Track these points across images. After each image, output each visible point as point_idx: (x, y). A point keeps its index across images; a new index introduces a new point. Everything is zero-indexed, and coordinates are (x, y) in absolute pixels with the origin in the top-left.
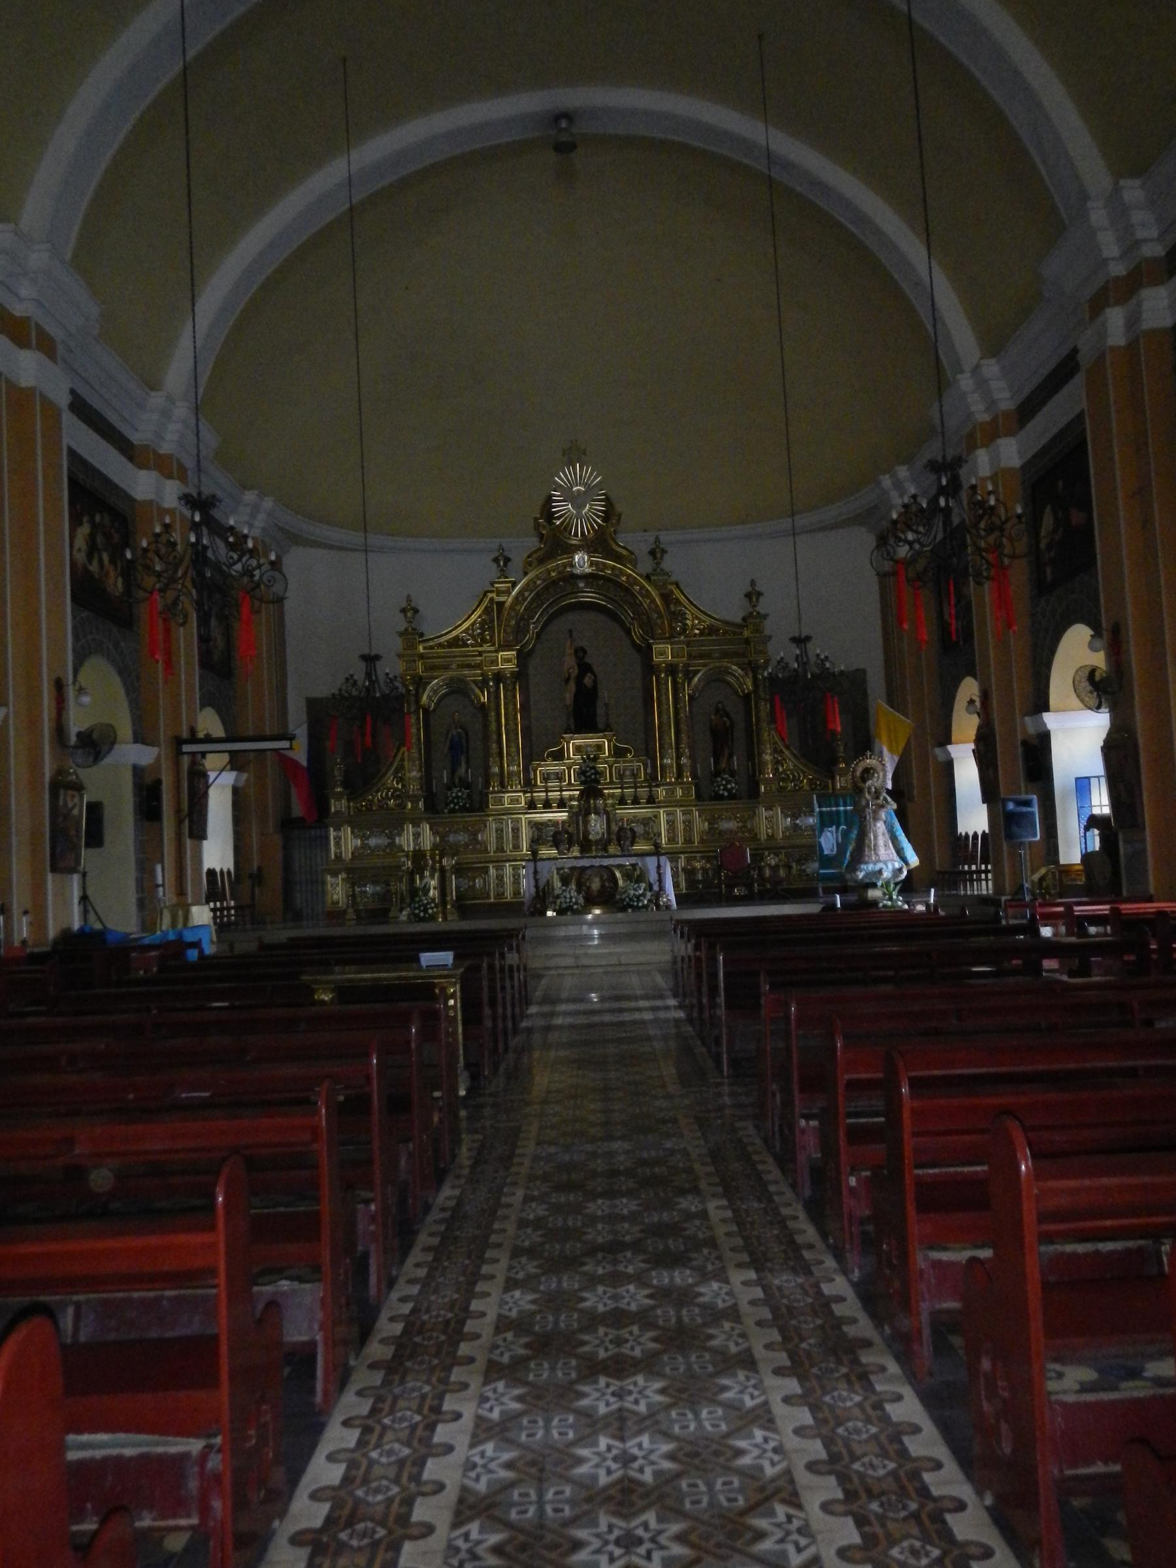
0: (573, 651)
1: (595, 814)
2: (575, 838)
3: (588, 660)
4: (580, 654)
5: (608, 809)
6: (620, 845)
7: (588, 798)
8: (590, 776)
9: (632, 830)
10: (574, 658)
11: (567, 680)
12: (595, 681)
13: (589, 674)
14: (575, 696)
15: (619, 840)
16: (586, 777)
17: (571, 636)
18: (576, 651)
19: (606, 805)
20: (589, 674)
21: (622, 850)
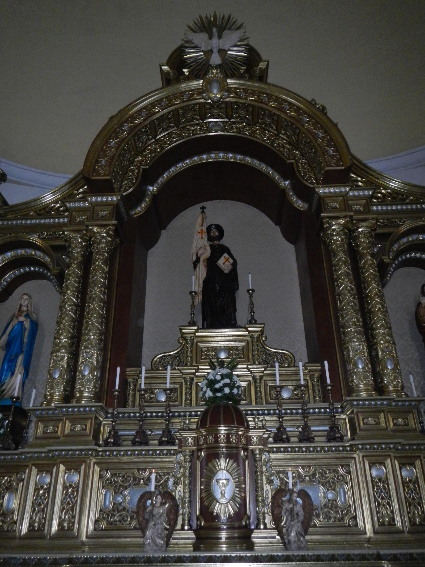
0: (205, 229)
1: (229, 456)
2: (184, 511)
3: (225, 241)
4: (215, 233)
5: (255, 448)
6: (279, 529)
7: (216, 422)
8: (221, 390)
9: (303, 494)
10: (205, 236)
11: (196, 264)
12: (235, 264)
13: (226, 255)
14: (205, 282)
15: (277, 519)
16: (215, 391)
17: (203, 212)
18: (209, 229)
19: (249, 440)
20: (226, 255)
21: (286, 544)
